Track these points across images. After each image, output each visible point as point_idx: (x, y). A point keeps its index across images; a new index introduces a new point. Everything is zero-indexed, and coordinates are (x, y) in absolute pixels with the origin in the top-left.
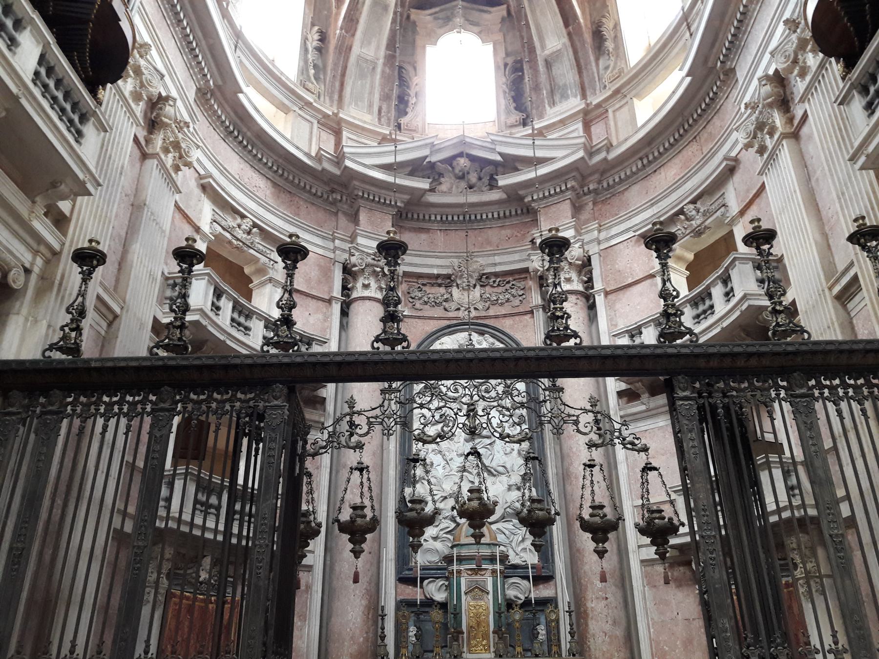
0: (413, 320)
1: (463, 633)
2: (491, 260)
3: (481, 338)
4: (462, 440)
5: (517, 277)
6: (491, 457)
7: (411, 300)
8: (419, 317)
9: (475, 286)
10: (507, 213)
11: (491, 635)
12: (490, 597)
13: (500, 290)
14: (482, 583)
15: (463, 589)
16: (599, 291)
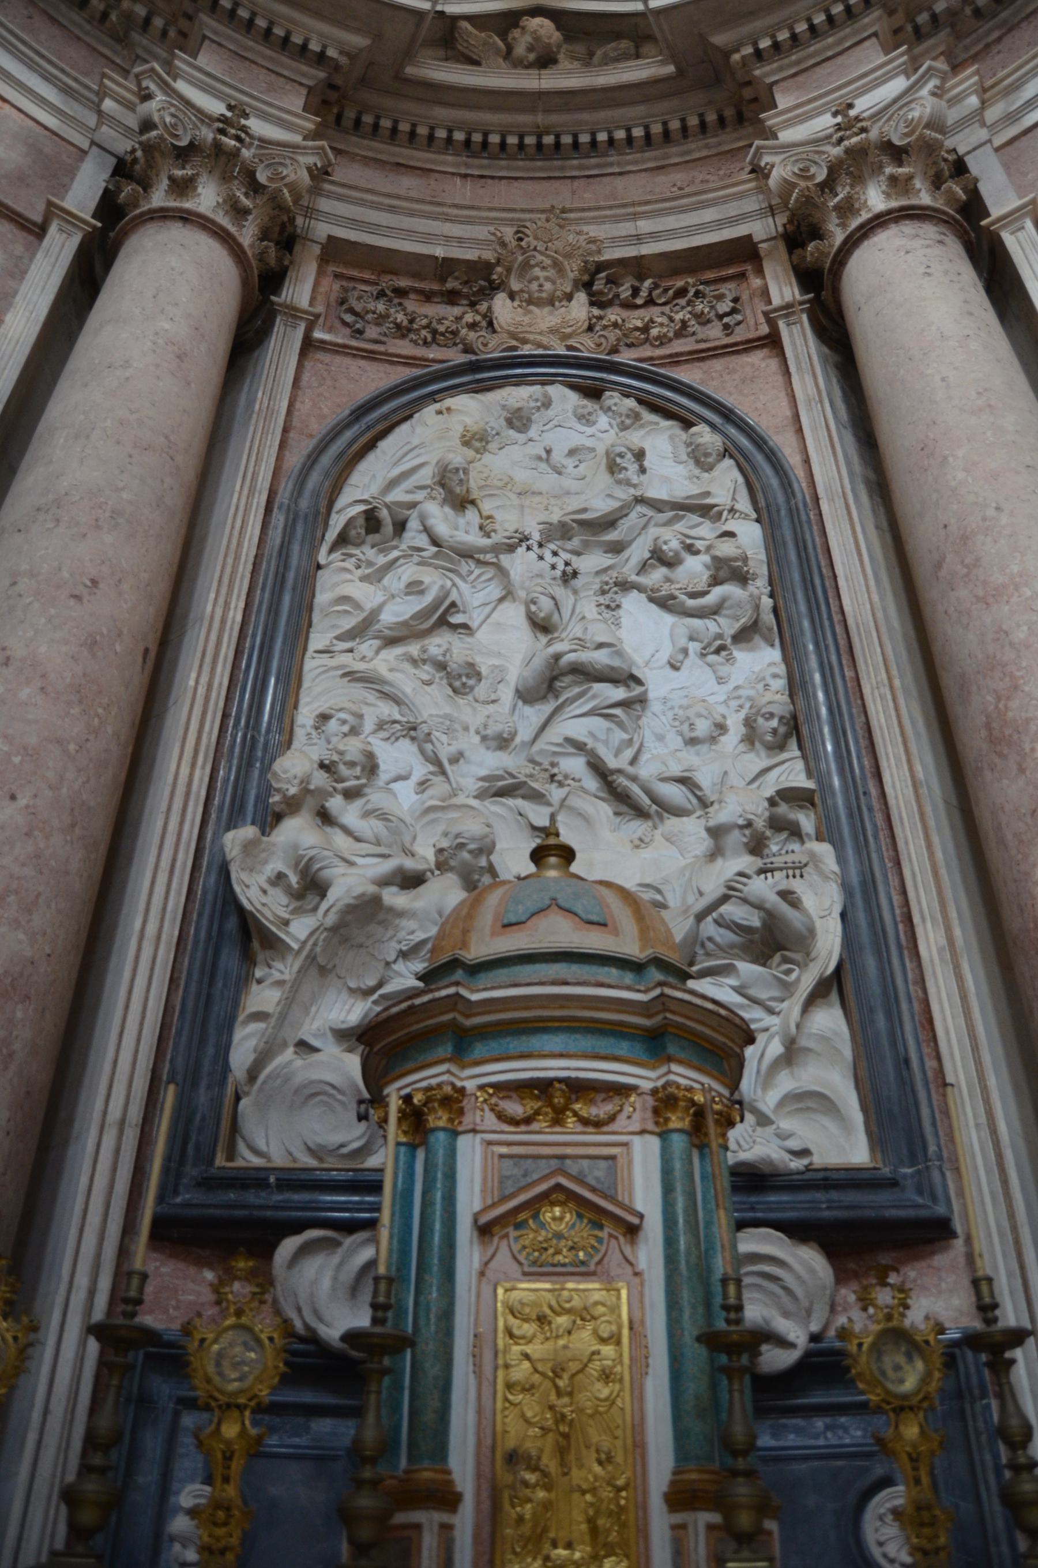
0: (347, 361)
1: (447, 1499)
2: (626, 228)
3: (589, 405)
4: (507, 694)
5: (710, 275)
6: (629, 753)
7: (349, 318)
8: (371, 356)
9: (569, 297)
10: (675, 125)
11: (660, 1520)
12: (649, 1255)
13: (655, 311)
14: (598, 1172)
15: (470, 1199)
16: (1012, 218)
